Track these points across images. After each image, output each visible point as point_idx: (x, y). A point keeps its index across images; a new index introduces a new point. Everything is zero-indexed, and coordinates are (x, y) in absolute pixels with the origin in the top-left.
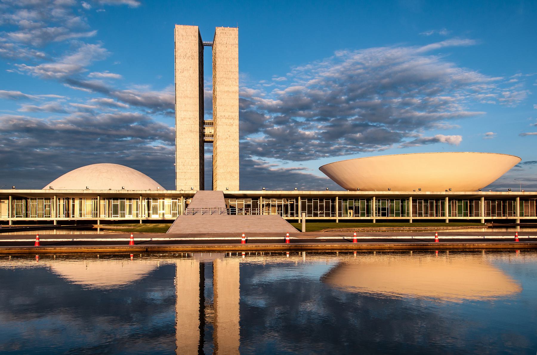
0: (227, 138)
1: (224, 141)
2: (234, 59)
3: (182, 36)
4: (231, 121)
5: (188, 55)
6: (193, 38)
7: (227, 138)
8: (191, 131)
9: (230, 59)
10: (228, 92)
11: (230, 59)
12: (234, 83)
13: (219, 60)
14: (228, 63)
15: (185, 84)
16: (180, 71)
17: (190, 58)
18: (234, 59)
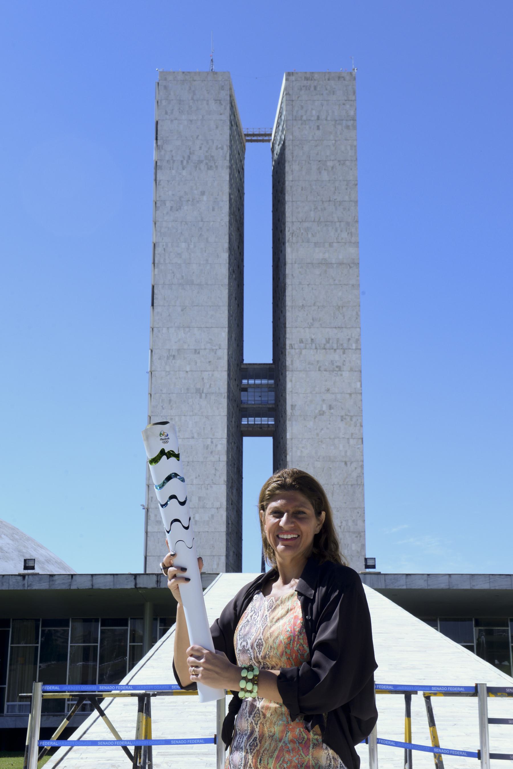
0: (322, 413)
1: (310, 424)
2: (342, 163)
3: (180, 102)
4: (336, 357)
5: (195, 158)
6: (213, 106)
7: (322, 413)
8: (199, 392)
9: (330, 164)
10: (326, 263)
11: (330, 164)
12: (344, 235)
13: (296, 167)
14: (325, 176)
15: (183, 245)
16: (168, 204)
17: (203, 166)
18: (342, 163)
